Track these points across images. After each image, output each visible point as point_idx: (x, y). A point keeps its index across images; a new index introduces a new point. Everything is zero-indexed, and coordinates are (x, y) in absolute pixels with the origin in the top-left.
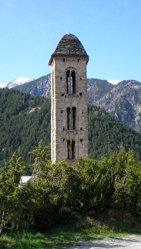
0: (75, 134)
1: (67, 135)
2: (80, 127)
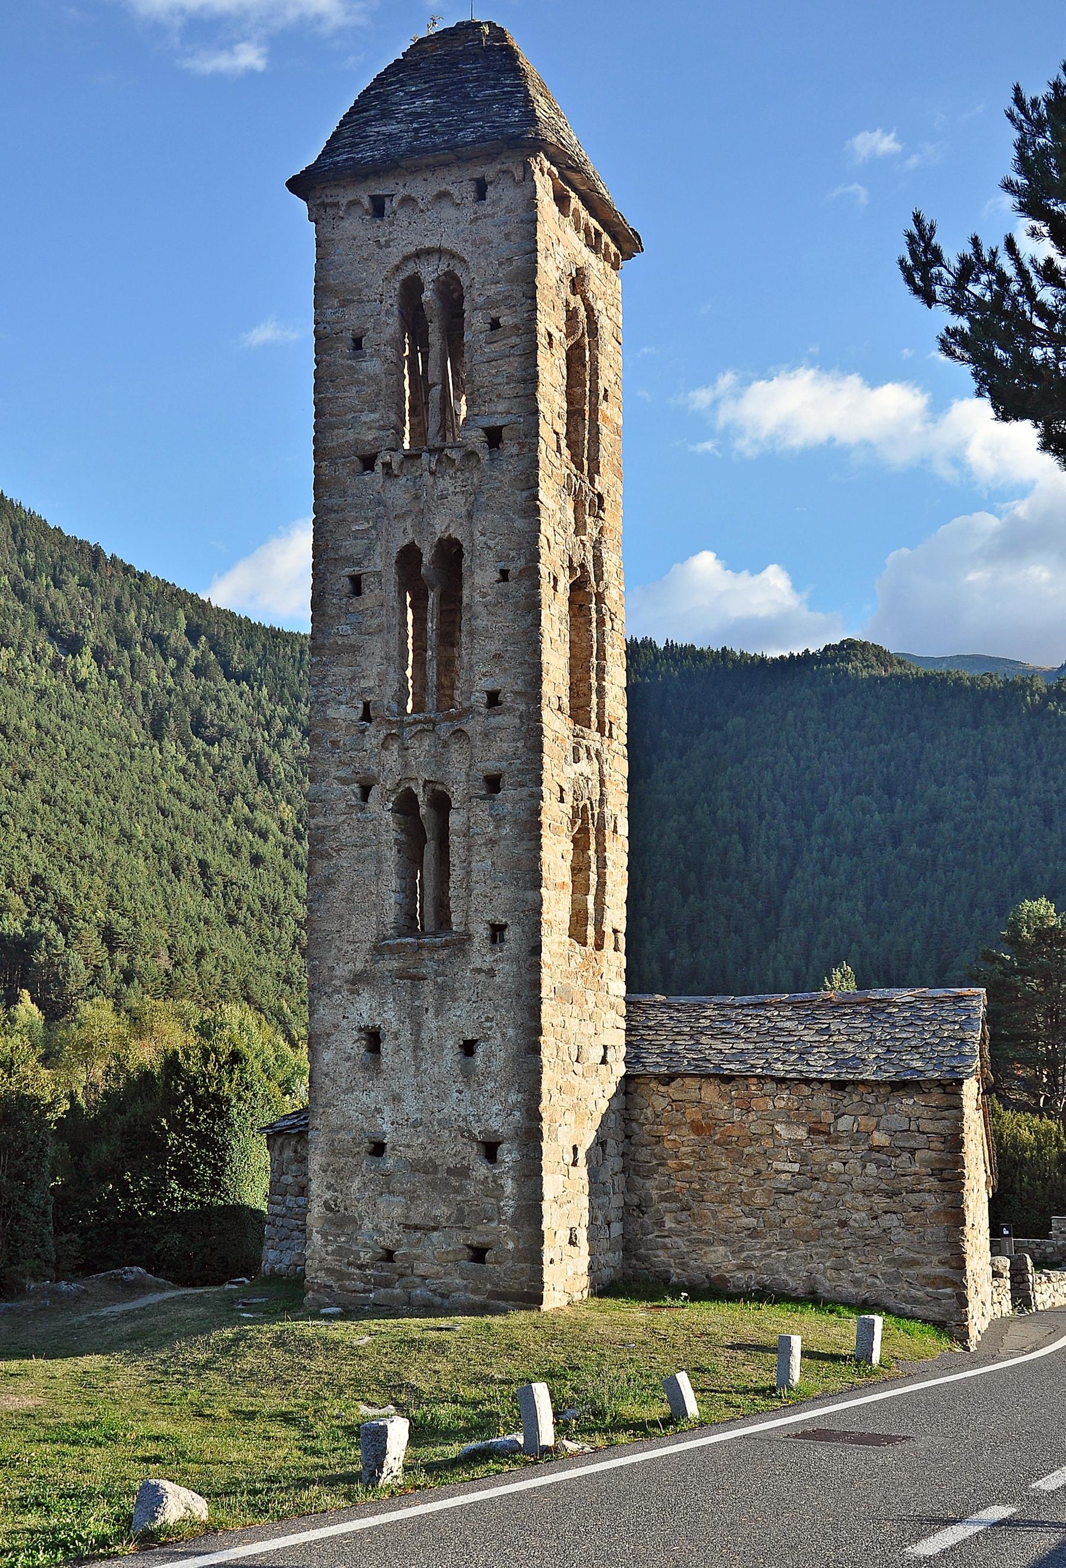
0: (445, 745)
1: (392, 758)
2: (487, 684)
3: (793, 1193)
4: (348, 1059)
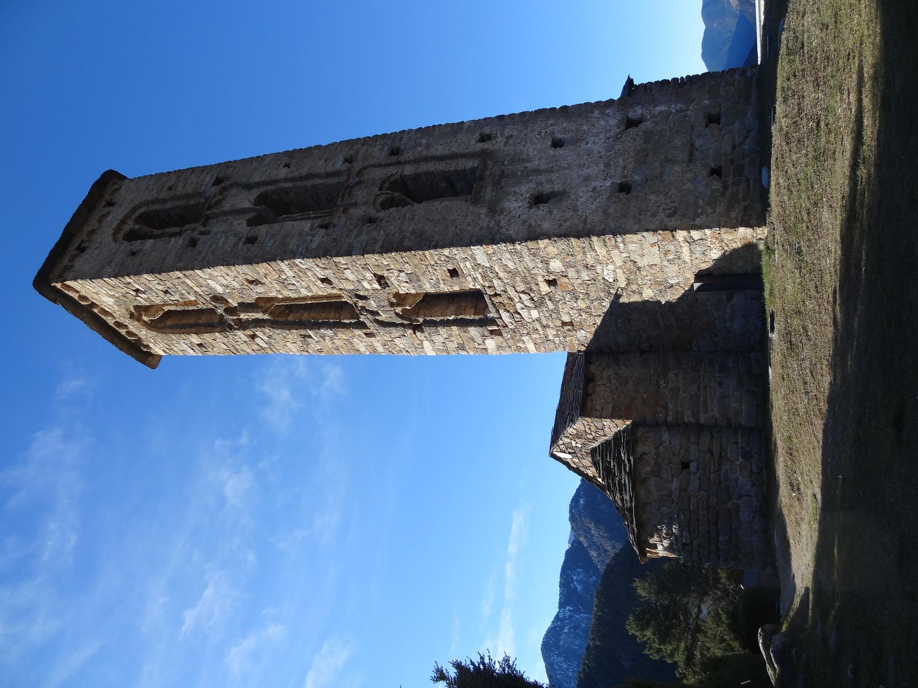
4: (551, 212)
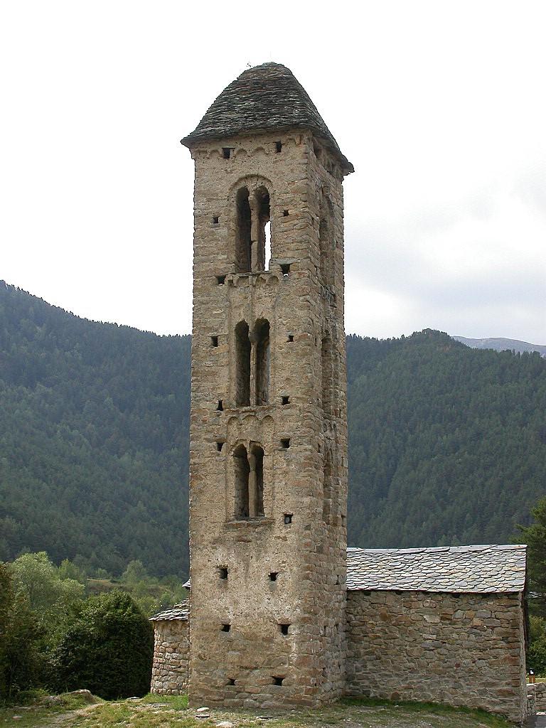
0: (261, 423)
1: (234, 428)
3: (432, 650)
4: (211, 582)
